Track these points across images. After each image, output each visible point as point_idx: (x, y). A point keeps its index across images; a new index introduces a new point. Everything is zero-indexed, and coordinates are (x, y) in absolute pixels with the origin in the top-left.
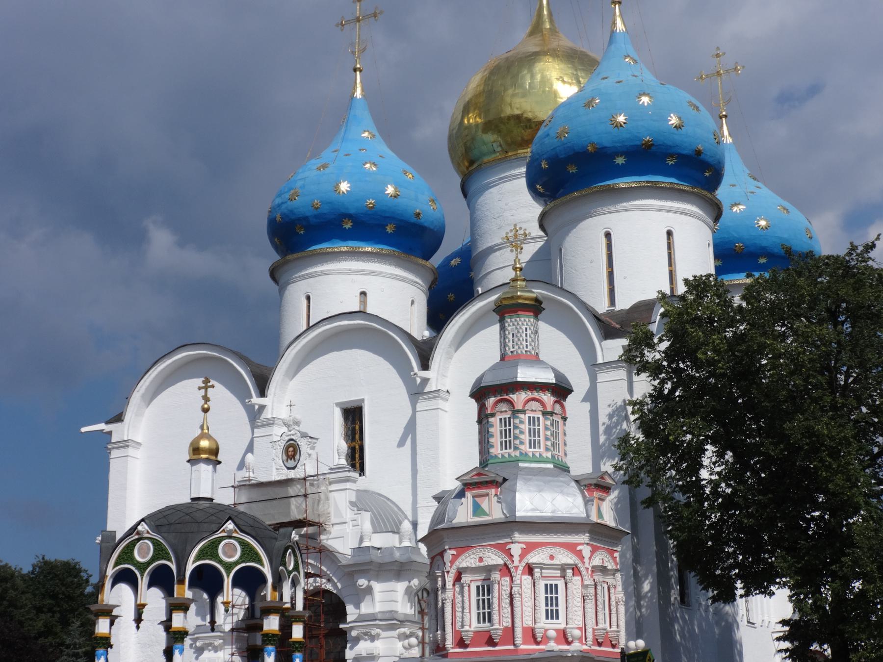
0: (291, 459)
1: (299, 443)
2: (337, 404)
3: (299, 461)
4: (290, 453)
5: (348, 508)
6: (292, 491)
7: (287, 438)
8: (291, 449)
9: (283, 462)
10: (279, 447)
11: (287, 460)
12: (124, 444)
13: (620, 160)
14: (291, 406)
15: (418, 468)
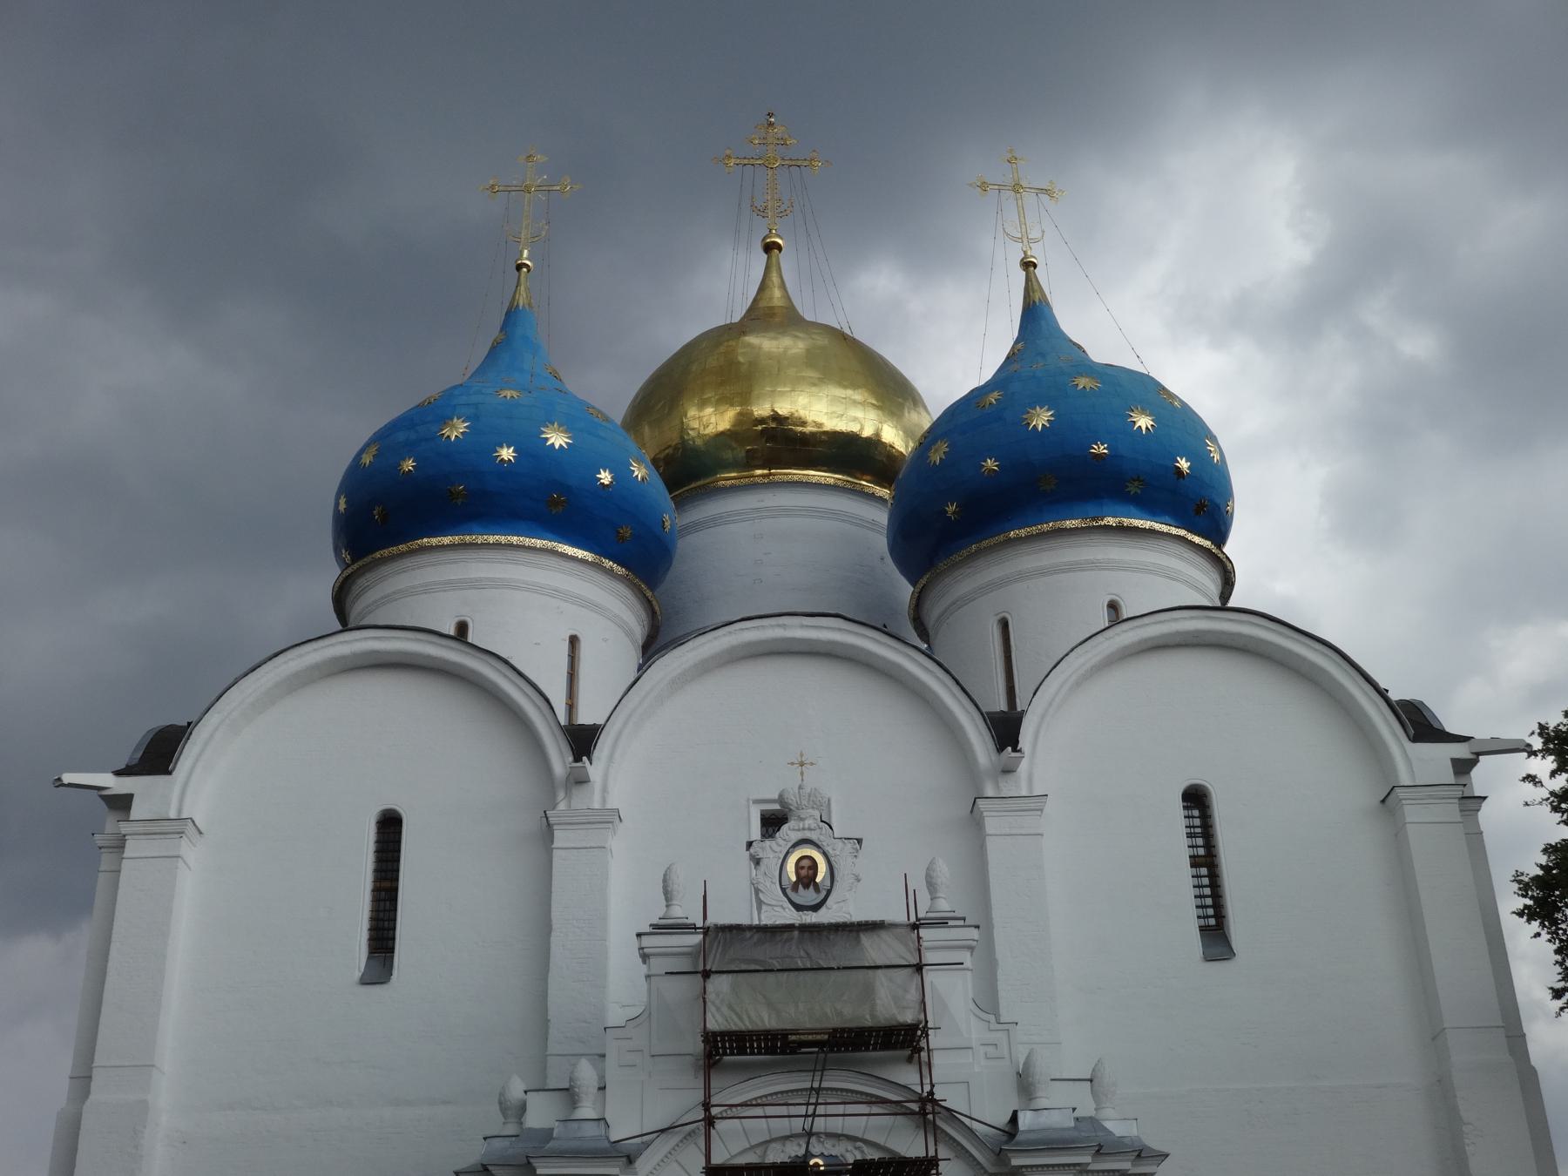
0: (806, 886)
1: (829, 849)
2: (757, 802)
3: (829, 892)
4: (803, 872)
5: (973, 1018)
6: (875, 949)
7: (795, 836)
8: (806, 863)
9: (784, 890)
10: (771, 855)
11: (795, 887)
12: (175, 827)
13: (1133, 489)
14: (802, 764)
15: (999, 956)
